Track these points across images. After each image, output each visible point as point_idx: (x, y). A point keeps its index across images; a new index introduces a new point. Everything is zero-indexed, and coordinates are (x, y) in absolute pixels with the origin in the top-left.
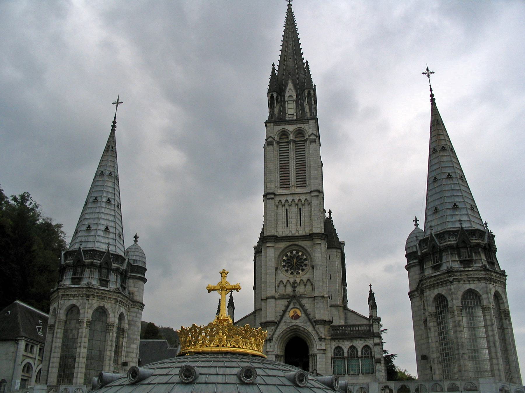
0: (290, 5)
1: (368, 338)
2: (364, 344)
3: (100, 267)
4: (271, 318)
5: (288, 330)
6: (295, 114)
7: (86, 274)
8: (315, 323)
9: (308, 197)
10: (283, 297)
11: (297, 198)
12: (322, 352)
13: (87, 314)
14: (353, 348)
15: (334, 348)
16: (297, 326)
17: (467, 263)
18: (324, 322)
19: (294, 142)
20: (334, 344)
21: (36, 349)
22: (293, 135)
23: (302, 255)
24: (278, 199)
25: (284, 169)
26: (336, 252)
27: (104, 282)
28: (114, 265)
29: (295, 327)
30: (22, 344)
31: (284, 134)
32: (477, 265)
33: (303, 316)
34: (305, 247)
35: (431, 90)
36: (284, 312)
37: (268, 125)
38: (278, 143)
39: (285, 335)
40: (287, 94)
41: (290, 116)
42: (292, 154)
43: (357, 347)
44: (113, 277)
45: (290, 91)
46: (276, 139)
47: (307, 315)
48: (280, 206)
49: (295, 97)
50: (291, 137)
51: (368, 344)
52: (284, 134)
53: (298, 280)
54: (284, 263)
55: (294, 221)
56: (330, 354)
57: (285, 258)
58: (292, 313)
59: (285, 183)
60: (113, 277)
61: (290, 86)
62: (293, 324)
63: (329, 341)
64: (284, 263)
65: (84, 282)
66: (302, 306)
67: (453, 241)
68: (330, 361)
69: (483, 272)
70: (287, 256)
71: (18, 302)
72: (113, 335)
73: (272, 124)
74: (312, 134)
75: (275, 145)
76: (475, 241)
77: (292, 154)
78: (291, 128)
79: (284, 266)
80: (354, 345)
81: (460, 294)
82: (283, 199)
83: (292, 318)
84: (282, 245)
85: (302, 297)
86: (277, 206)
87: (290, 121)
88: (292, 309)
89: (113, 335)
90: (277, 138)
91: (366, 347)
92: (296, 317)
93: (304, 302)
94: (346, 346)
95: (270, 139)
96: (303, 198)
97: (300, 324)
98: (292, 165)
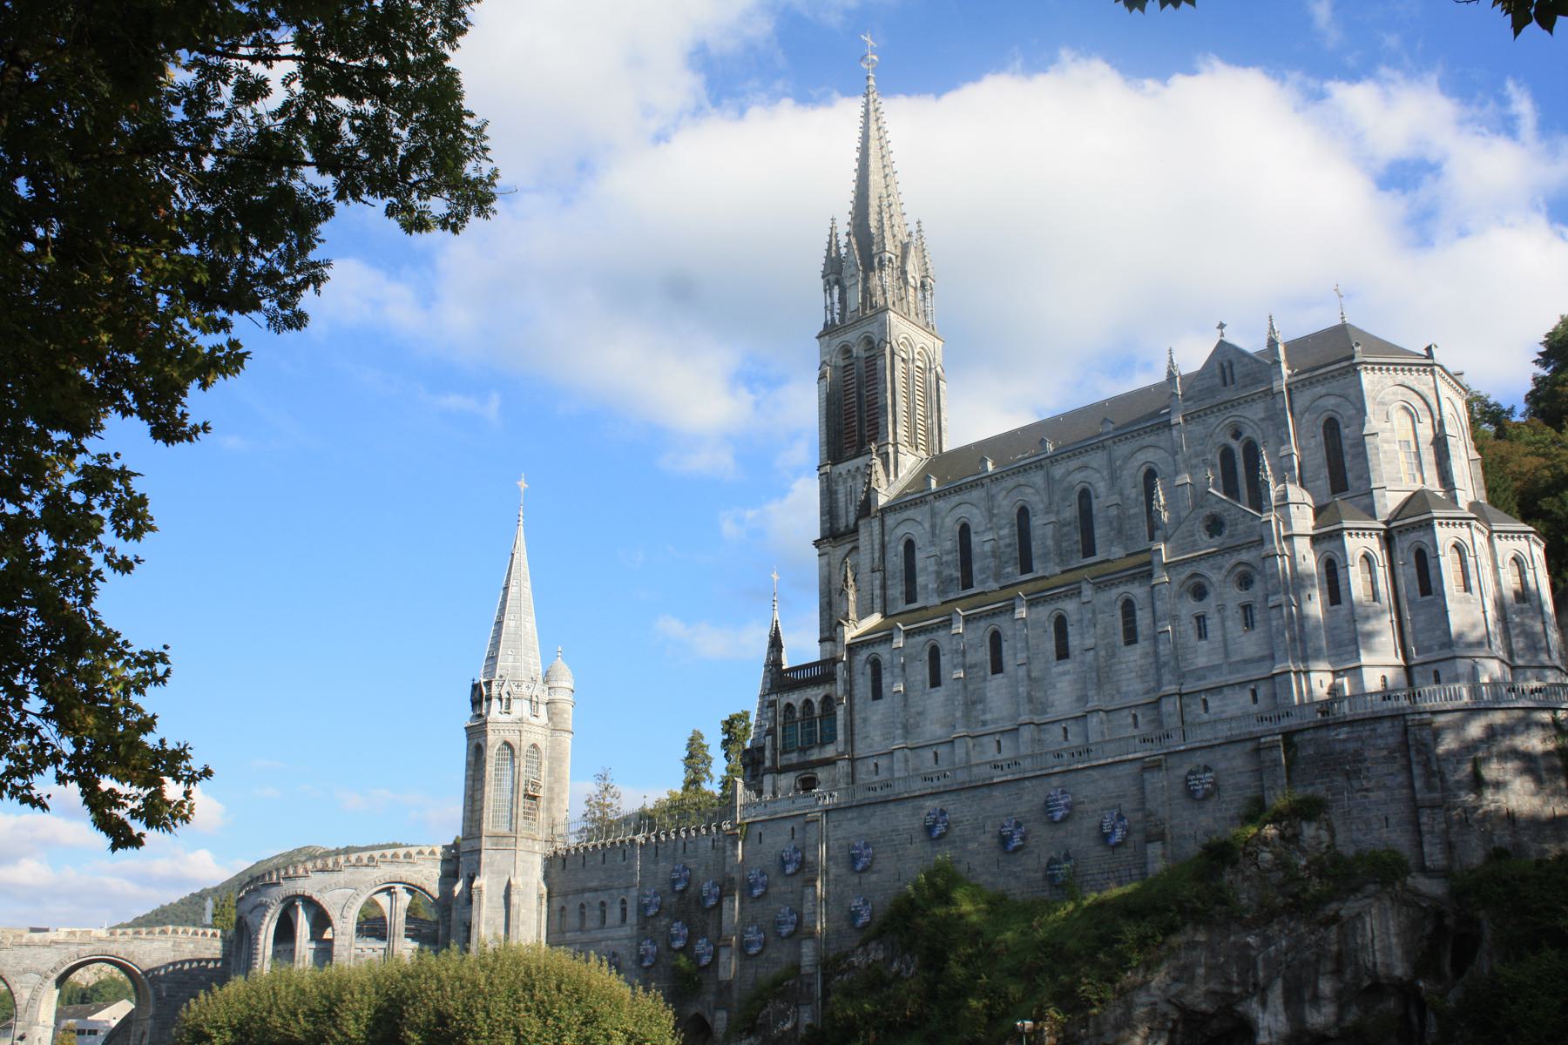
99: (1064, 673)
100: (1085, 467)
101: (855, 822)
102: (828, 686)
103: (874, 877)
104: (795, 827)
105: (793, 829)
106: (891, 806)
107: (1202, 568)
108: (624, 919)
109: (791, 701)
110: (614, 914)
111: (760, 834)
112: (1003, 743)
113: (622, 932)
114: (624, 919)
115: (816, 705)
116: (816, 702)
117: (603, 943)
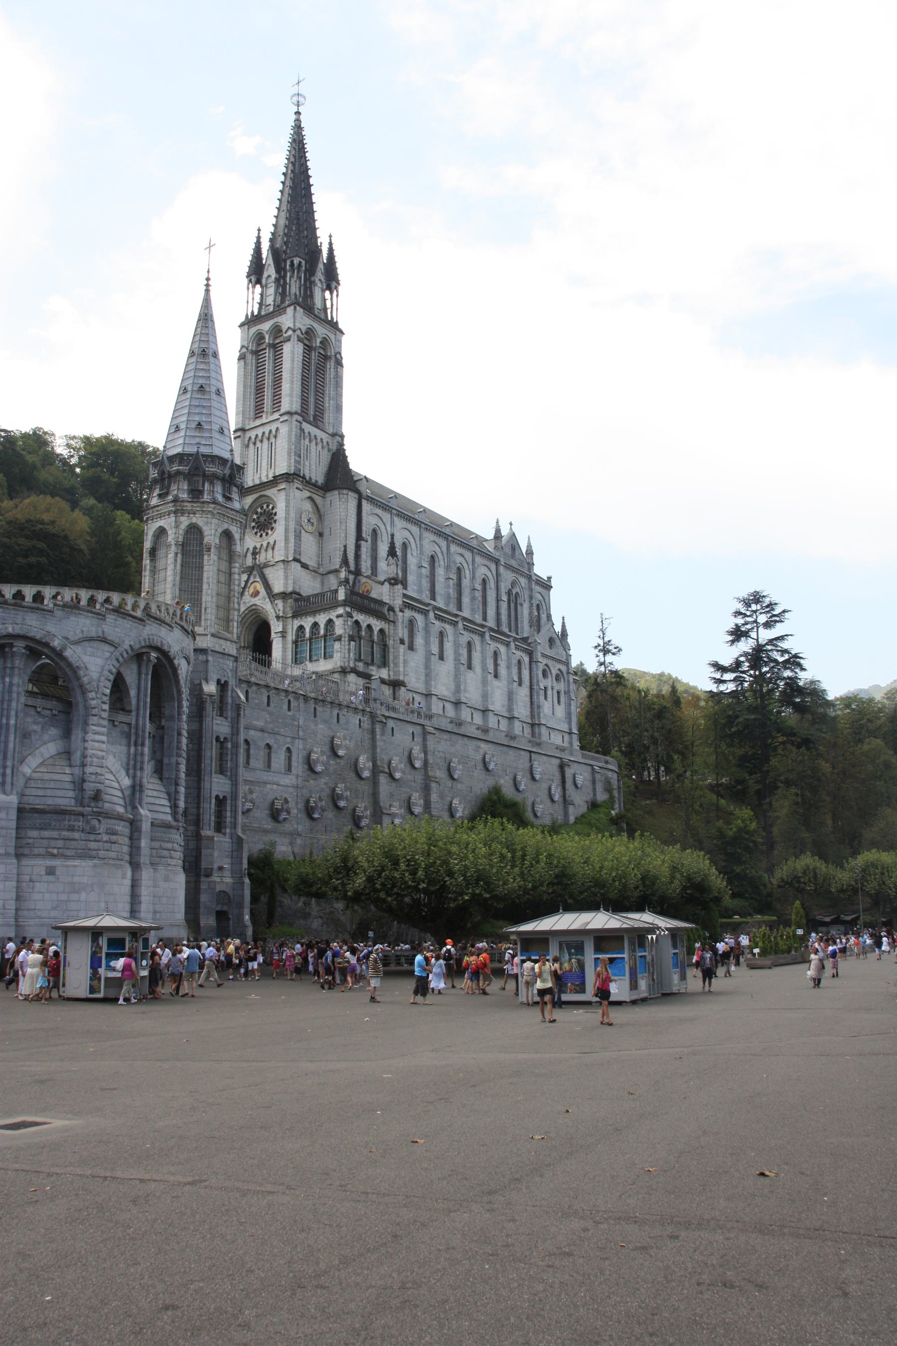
0: (298, 113)
1: (331, 608)
2: (327, 618)
5: (246, 612)
6: (272, 303)
11: (266, 429)
12: (279, 635)
14: (315, 625)
15: (295, 627)
16: (256, 605)
20: (297, 623)
22: (269, 337)
23: (273, 508)
24: (248, 435)
25: (259, 390)
26: (339, 494)
29: (254, 607)
32: (170, 498)
34: (273, 497)
35: (208, 272)
37: (242, 328)
38: (256, 353)
39: (245, 619)
40: (265, 275)
41: (267, 308)
42: (269, 366)
43: (320, 623)
46: (250, 348)
48: (251, 445)
51: (332, 617)
52: (260, 337)
53: (265, 545)
54: (253, 524)
56: (291, 637)
57: (255, 517)
58: (252, 590)
59: (259, 411)
62: (252, 603)
63: (290, 619)
64: (253, 524)
68: (290, 645)
69: (171, 505)
70: (257, 513)
73: (246, 327)
74: (289, 328)
75: (249, 356)
77: (269, 366)
78: (266, 326)
79: (254, 527)
80: (317, 620)
83: (251, 596)
85: (266, 565)
86: (248, 446)
87: (266, 315)
88: (252, 583)
91: (330, 621)
92: (256, 594)
94: (307, 623)
95: (244, 350)
97: (258, 603)
98: (268, 380)
99: (499, 687)
100: (462, 555)
101: (448, 743)
102: (383, 622)
103: (459, 786)
104: (415, 733)
105: (413, 733)
106: (465, 739)
107: (550, 663)
108: (289, 768)
109: (360, 620)
110: (278, 760)
111: (393, 728)
112: (474, 715)
113: (288, 780)
114: (289, 768)
115: (376, 633)
116: (376, 630)
117: (269, 786)
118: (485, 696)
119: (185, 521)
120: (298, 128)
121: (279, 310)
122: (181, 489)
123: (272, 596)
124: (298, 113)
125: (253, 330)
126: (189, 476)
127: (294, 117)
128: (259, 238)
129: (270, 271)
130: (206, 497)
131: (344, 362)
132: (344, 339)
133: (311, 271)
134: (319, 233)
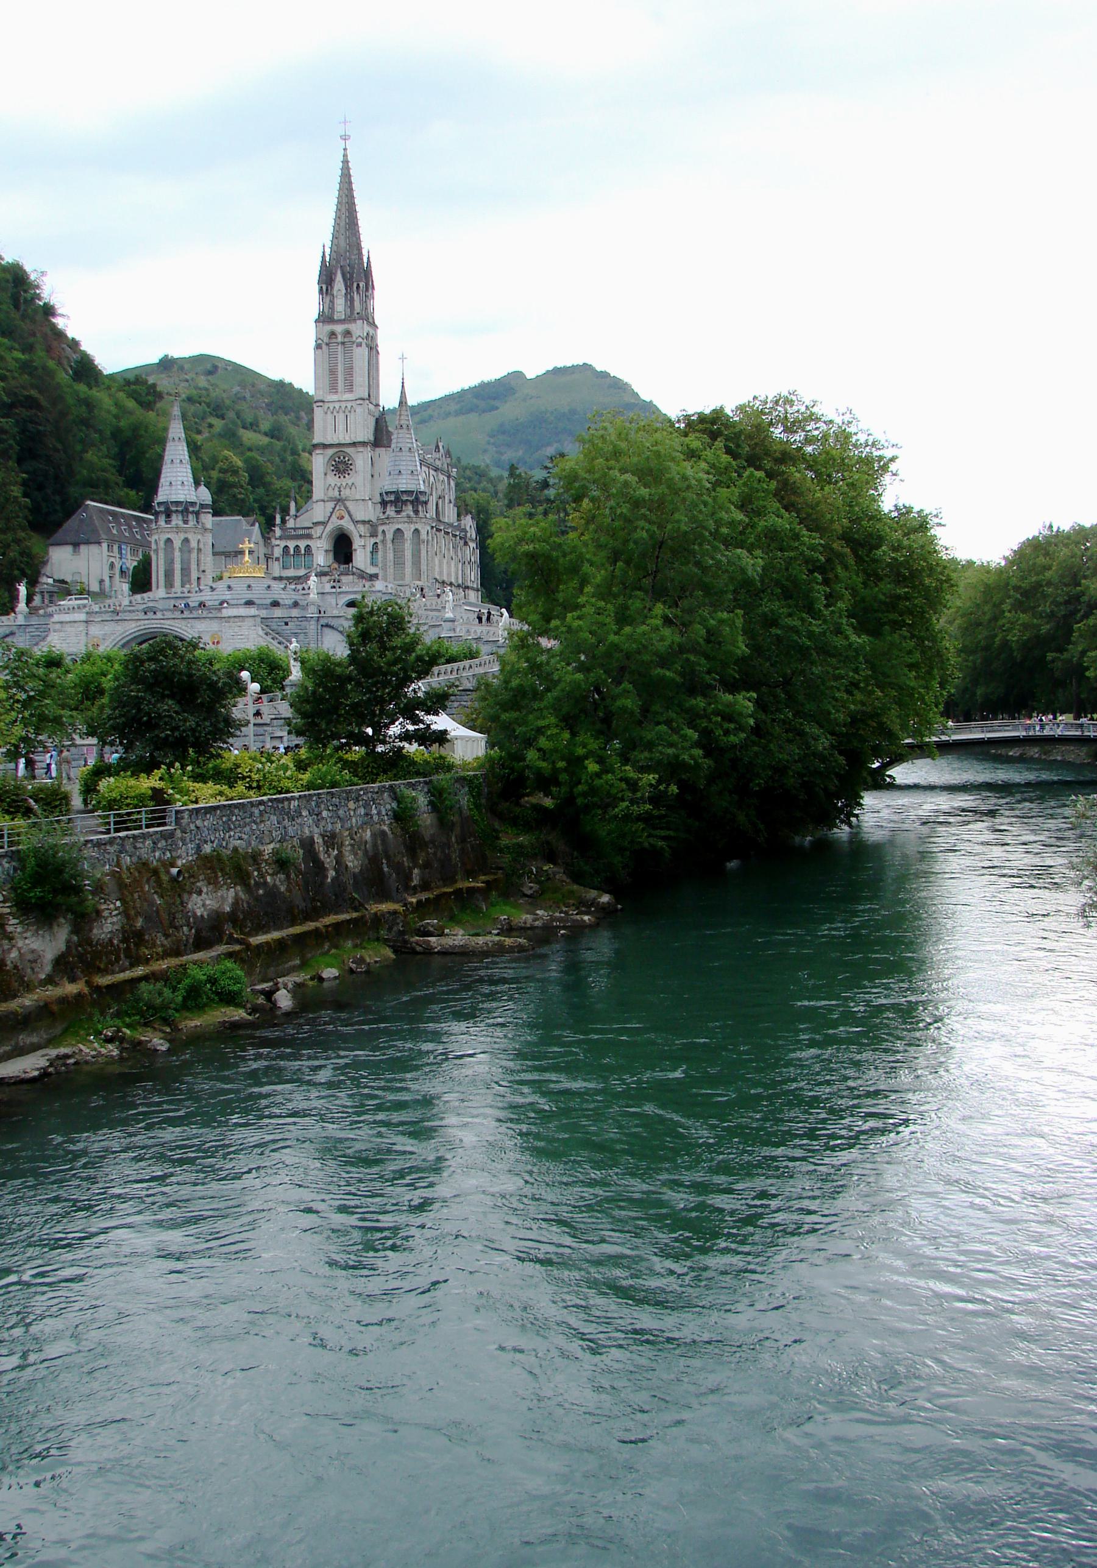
0: (345, 149)
3: (182, 512)
4: (321, 519)
7: (174, 517)
8: (356, 522)
9: (354, 404)
10: (331, 499)
11: (343, 405)
13: (177, 543)
17: (398, 512)
18: (364, 522)
19: (343, 343)
21: (116, 547)
24: (326, 405)
25: (333, 372)
27: (186, 522)
28: (191, 509)
30: (105, 545)
31: (333, 334)
32: (404, 514)
33: (347, 516)
36: (332, 513)
38: (327, 344)
44: (191, 517)
45: (339, 284)
47: (350, 515)
49: (344, 291)
50: (340, 339)
52: (333, 334)
55: (341, 427)
56: (369, 548)
59: (333, 388)
60: (191, 517)
61: (339, 277)
65: (174, 523)
66: (346, 508)
67: (392, 498)
68: (369, 554)
71: (89, 502)
72: (194, 555)
75: (324, 346)
76: (405, 498)
78: (339, 328)
81: (392, 531)
82: (331, 406)
84: (330, 452)
89: (194, 555)
90: (326, 340)
92: (342, 518)
93: (348, 504)
96: (349, 405)
118: (449, 575)
119: (413, 527)
120: (346, 162)
121: (350, 318)
122: (409, 510)
123: (356, 522)
124: (345, 149)
125: (329, 328)
126: (412, 502)
127: (342, 152)
128: (324, 253)
129: (339, 284)
130: (421, 514)
131: (379, 349)
132: (379, 331)
133: (367, 290)
134: (365, 252)
